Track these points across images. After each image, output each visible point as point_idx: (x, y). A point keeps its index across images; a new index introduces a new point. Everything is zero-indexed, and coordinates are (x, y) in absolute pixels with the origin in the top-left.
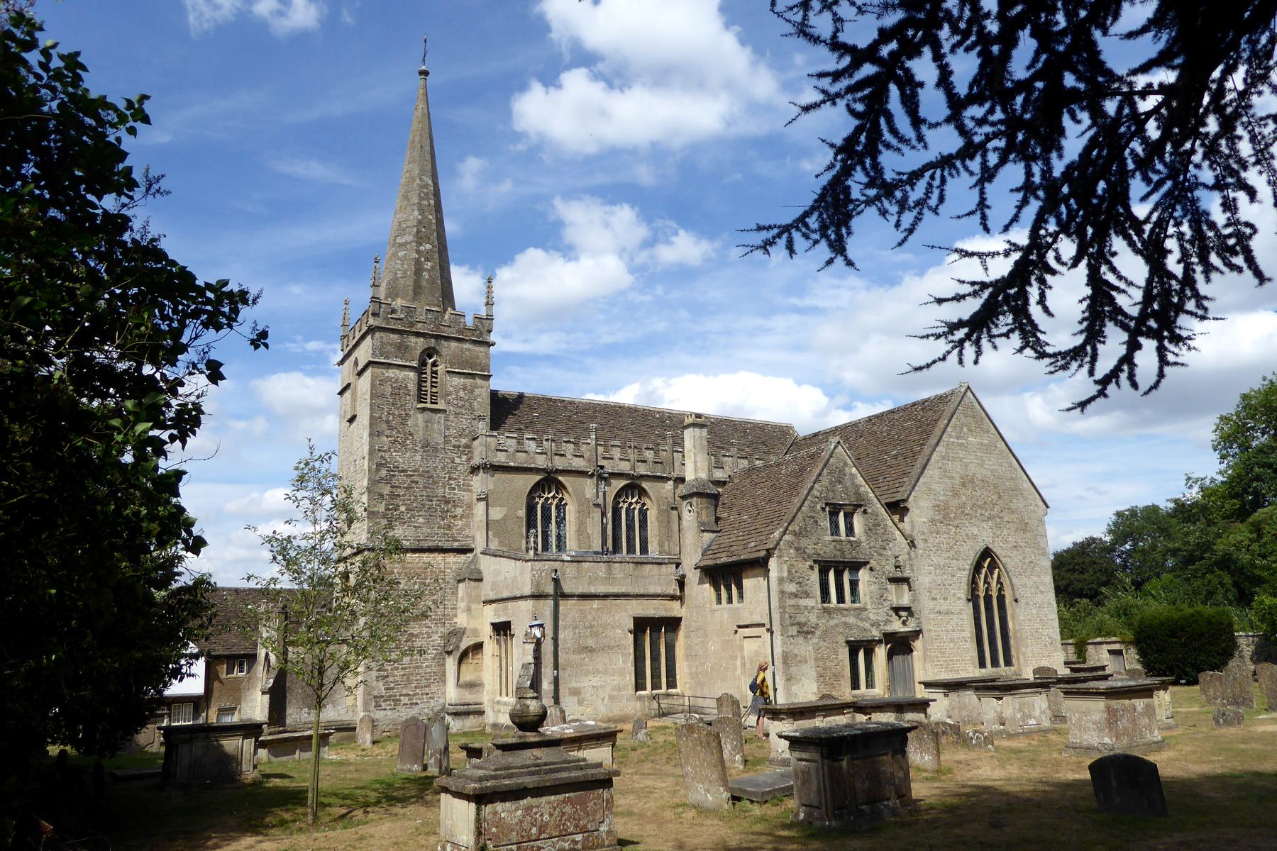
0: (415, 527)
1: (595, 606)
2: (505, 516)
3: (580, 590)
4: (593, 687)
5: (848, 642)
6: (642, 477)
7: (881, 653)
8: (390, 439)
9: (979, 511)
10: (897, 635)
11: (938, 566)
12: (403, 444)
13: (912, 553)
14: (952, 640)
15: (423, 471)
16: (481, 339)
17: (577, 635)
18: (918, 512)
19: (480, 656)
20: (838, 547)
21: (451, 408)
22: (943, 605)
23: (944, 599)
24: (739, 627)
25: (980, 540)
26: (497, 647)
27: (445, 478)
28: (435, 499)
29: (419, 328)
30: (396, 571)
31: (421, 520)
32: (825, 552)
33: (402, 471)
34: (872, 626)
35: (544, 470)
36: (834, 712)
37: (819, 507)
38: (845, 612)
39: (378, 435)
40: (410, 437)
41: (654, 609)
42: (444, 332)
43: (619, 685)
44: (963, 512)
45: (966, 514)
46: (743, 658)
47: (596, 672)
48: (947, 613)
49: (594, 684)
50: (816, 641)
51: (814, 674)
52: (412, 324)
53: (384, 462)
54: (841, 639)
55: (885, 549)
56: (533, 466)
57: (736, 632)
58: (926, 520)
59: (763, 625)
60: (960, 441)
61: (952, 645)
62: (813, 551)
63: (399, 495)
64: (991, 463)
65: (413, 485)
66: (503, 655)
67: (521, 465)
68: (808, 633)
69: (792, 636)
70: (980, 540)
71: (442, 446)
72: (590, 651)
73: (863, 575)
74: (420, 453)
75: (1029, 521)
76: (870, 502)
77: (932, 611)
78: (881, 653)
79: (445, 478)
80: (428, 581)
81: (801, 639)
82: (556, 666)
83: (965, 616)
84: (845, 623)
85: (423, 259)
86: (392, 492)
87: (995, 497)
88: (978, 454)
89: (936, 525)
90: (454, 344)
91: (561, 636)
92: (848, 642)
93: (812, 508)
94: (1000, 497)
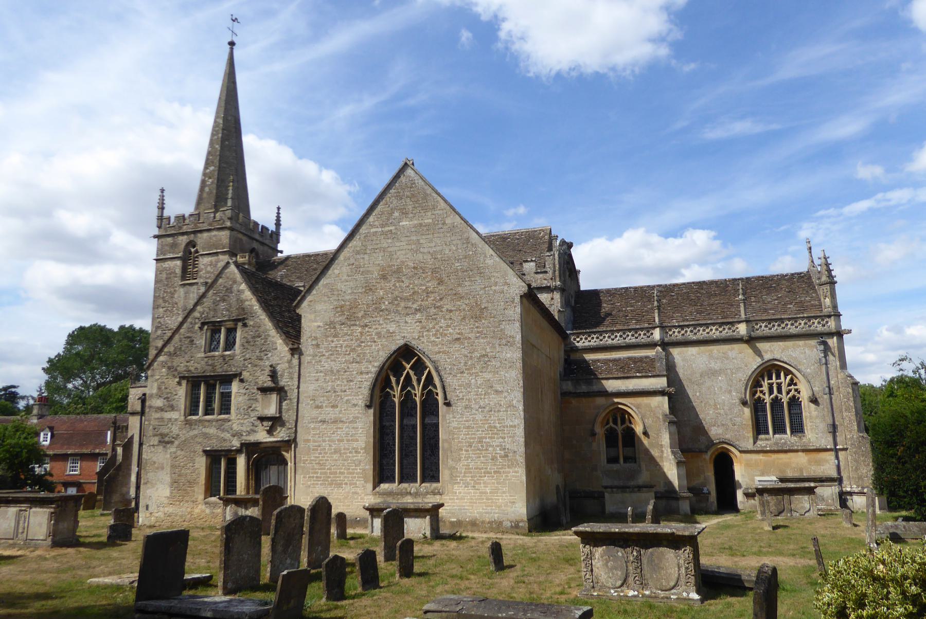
5: (205, 451)
7: (241, 462)
8: (164, 309)
9: (402, 304)
10: (262, 446)
12: (171, 311)
16: (224, 226)
18: (312, 316)
20: (210, 362)
23: (332, 407)
29: (185, 229)
32: (196, 368)
34: (234, 436)
38: (207, 424)
40: (176, 306)
44: (376, 308)
48: (335, 422)
50: (174, 450)
52: (180, 228)
54: (199, 449)
55: (261, 359)
58: (321, 324)
60: (387, 229)
61: (335, 456)
64: (433, 244)
68: (168, 443)
69: (153, 445)
70: (398, 337)
73: (235, 387)
76: (252, 314)
77: (314, 420)
78: (241, 462)
81: (160, 448)
82: (139, 465)
85: (207, 179)
88: (414, 238)
90: (205, 235)
92: (205, 451)
93: (190, 330)
94: (441, 282)
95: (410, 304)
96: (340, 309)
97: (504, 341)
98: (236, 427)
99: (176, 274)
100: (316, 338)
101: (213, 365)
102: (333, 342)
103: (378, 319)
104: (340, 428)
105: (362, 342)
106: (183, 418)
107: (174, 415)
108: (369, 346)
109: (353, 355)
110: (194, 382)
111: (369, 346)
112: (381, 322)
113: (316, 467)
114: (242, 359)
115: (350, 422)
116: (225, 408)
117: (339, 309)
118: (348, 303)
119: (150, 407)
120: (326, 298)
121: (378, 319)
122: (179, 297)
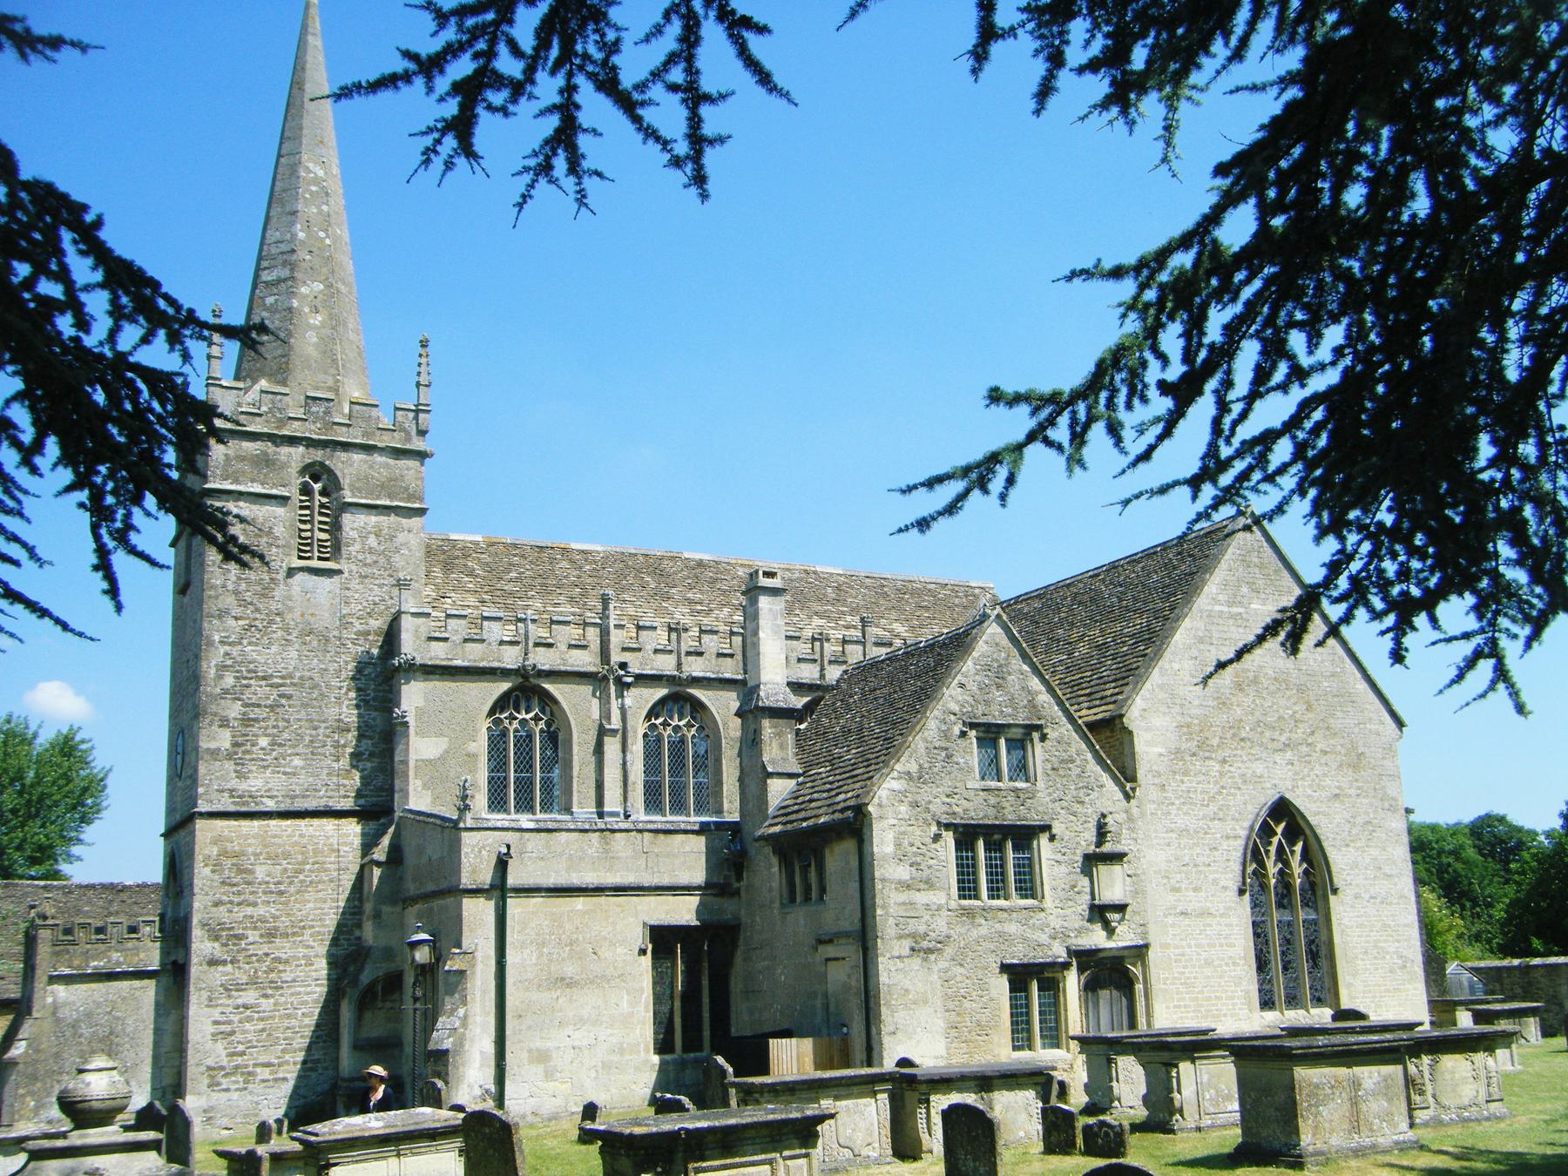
0: (285, 773)
1: (580, 907)
2: (446, 752)
3: (551, 880)
5: (1005, 968)
7: (1072, 982)
8: (241, 623)
9: (1267, 734)
10: (1102, 955)
11: (1184, 832)
12: (264, 631)
13: (1135, 811)
14: (1208, 963)
15: (301, 678)
19: (396, 996)
20: (993, 801)
21: (354, 568)
22: (1193, 901)
23: (1196, 890)
24: (820, 942)
25: (1268, 785)
27: (340, 688)
28: (323, 725)
30: (250, 850)
31: (297, 762)
33: (264, 678)
35: (516, 672)
36: (855, 1090)
37: (956, 730)
39: (220, 617)
40: (278, 619)
42: (337, 435)
43: (622, 1044)
45: (1242, 740)
47: (580, 1022)
49: (577, 1043)
50: (946, 964)
51: (939, 1023)
53: (229, 662)
56: (496, 664)
58: (1162, 750)
60: (1235, 610)
61: (1208, 971)
62: (945, 808)
63: (255, 720)
65: (283, 701)
67: (477, 664)
68: (930, 951)
69: (899, 957)
70: (1268, 785)
71: (336, 633)
72: (569, 985)
74: (297, 646)
75: (1367, 750)
78: (1072, 982)
79: (340, 688)
80: (308, 867)
81: (916, 962)
83: (1234, 920)
84: (1001, 934)
85: (307, 310)
86: (244, 714)
87: (1300, 708)
89: (1183, 759)
90: (358, 457)
92: (1005, 968)
94: (1309, 708)
95: (1276, 735)
96: (1185, 728)
97: (1386, 805)
98: (1056, 923)
99: (277, 538)
100: (1159, 775)
101: (998, 807)
102: (1182, 782)
103: (1239, 752)
104: (1210, 925)
105: (1223, 787)
106: (953, 904)
107: (938, 898)
108: (1232, 795)
109: (1213, 808)
110: (966, 836)
111: (1232, 795)
112: (1245, 758)
113: (1182, 989)
114: (1048, 799)
115: (1222, 915)
116: (1028, 886)
117: (1185, 730)
118: (1196, 721)
119: (883, 880)
120: (1163, 709)
121: (1239, 752)
122: (290, 598)
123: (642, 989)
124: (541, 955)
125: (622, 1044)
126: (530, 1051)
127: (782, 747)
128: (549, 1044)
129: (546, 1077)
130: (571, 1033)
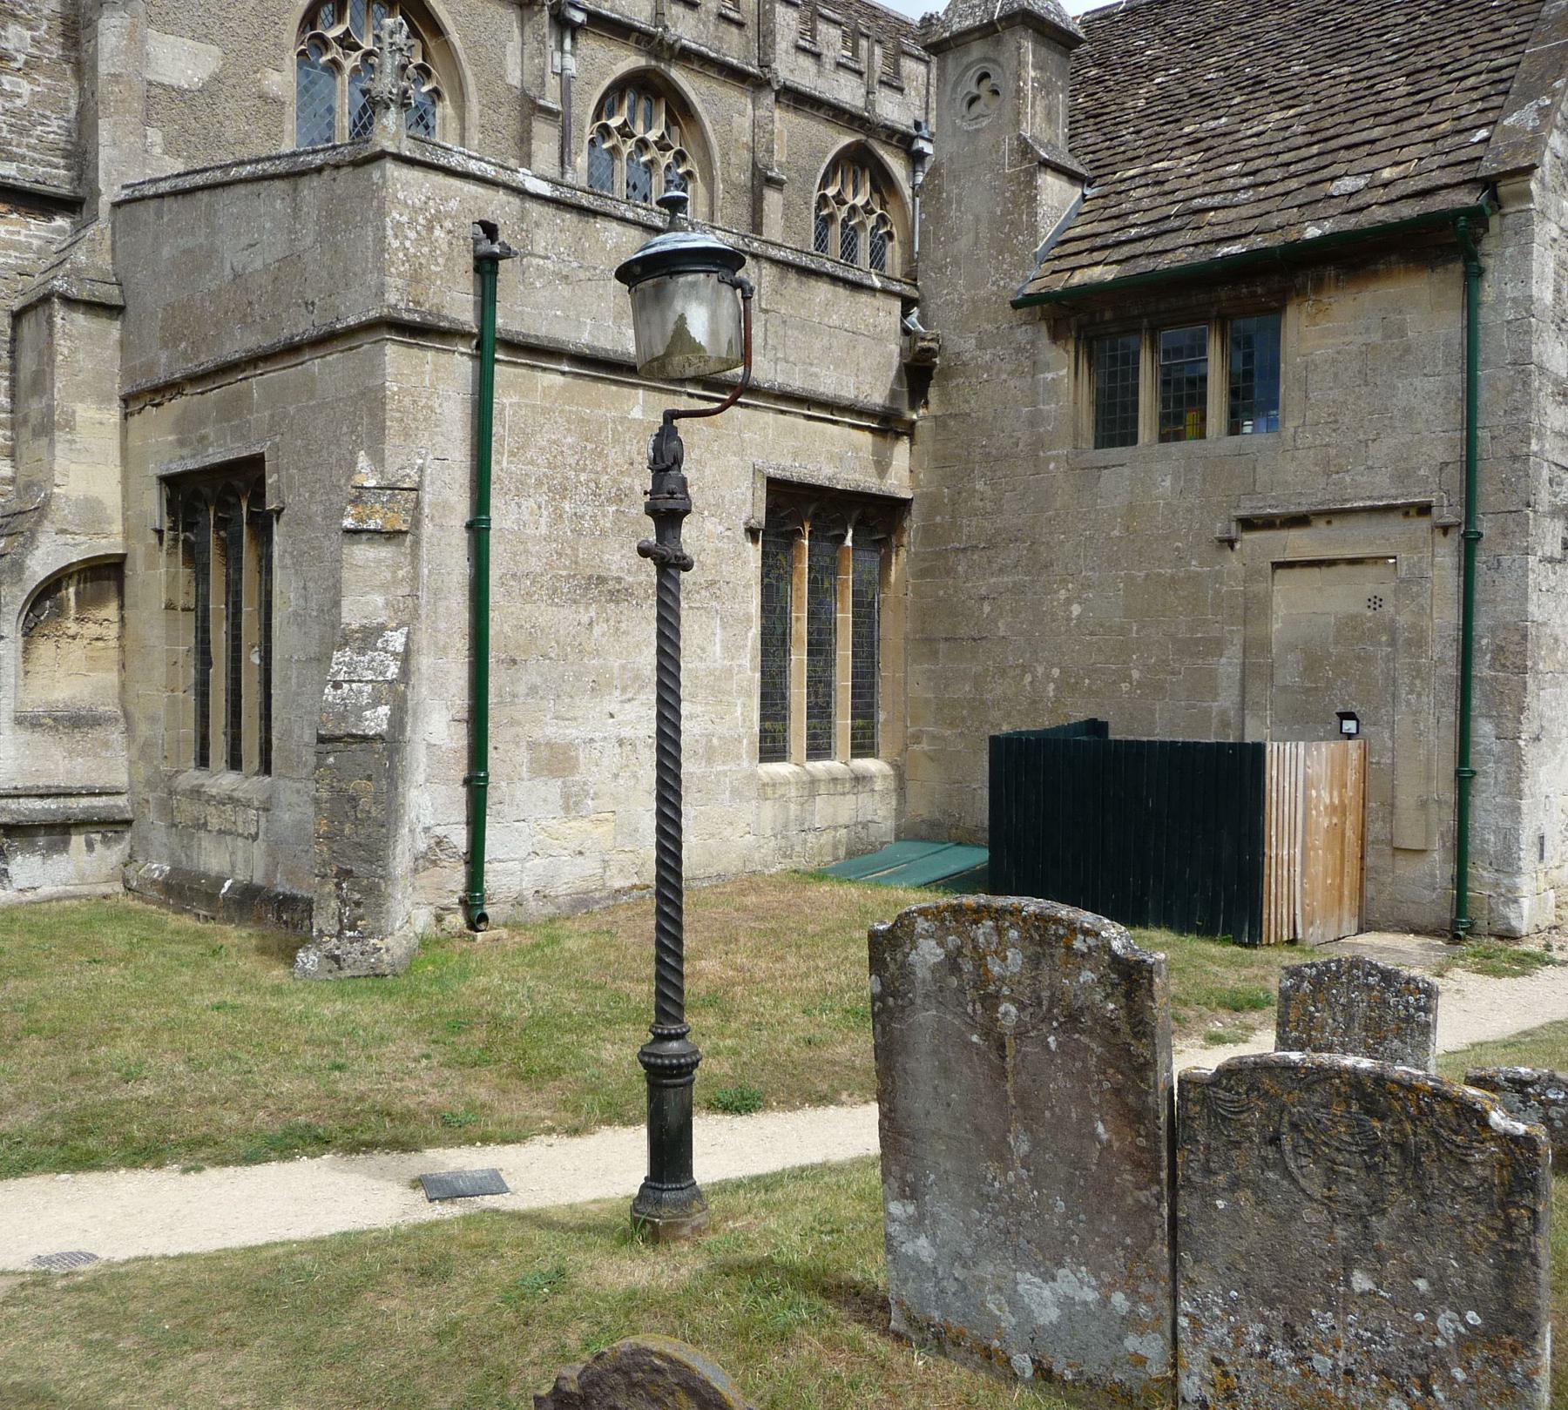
1: (636, 413)
2: (216, 79)
4: (621, 743)
6: (686, 56)
17: (566, 527)
24: (1248, 524)
26: (184, 573)
41: (831, 457)
46: (1256, 647)
49: (627, 732)
57: (1231, 543)
59: (1424, 510)
66: (217, 605)
91: (502, 516)
123: (748, 618)
124: (558, 516)
125: (709, 736)
126: (533, 746)
127: (1050, 117)
128: (572, 732)
129: (567, 809)
130: (614, 707)
